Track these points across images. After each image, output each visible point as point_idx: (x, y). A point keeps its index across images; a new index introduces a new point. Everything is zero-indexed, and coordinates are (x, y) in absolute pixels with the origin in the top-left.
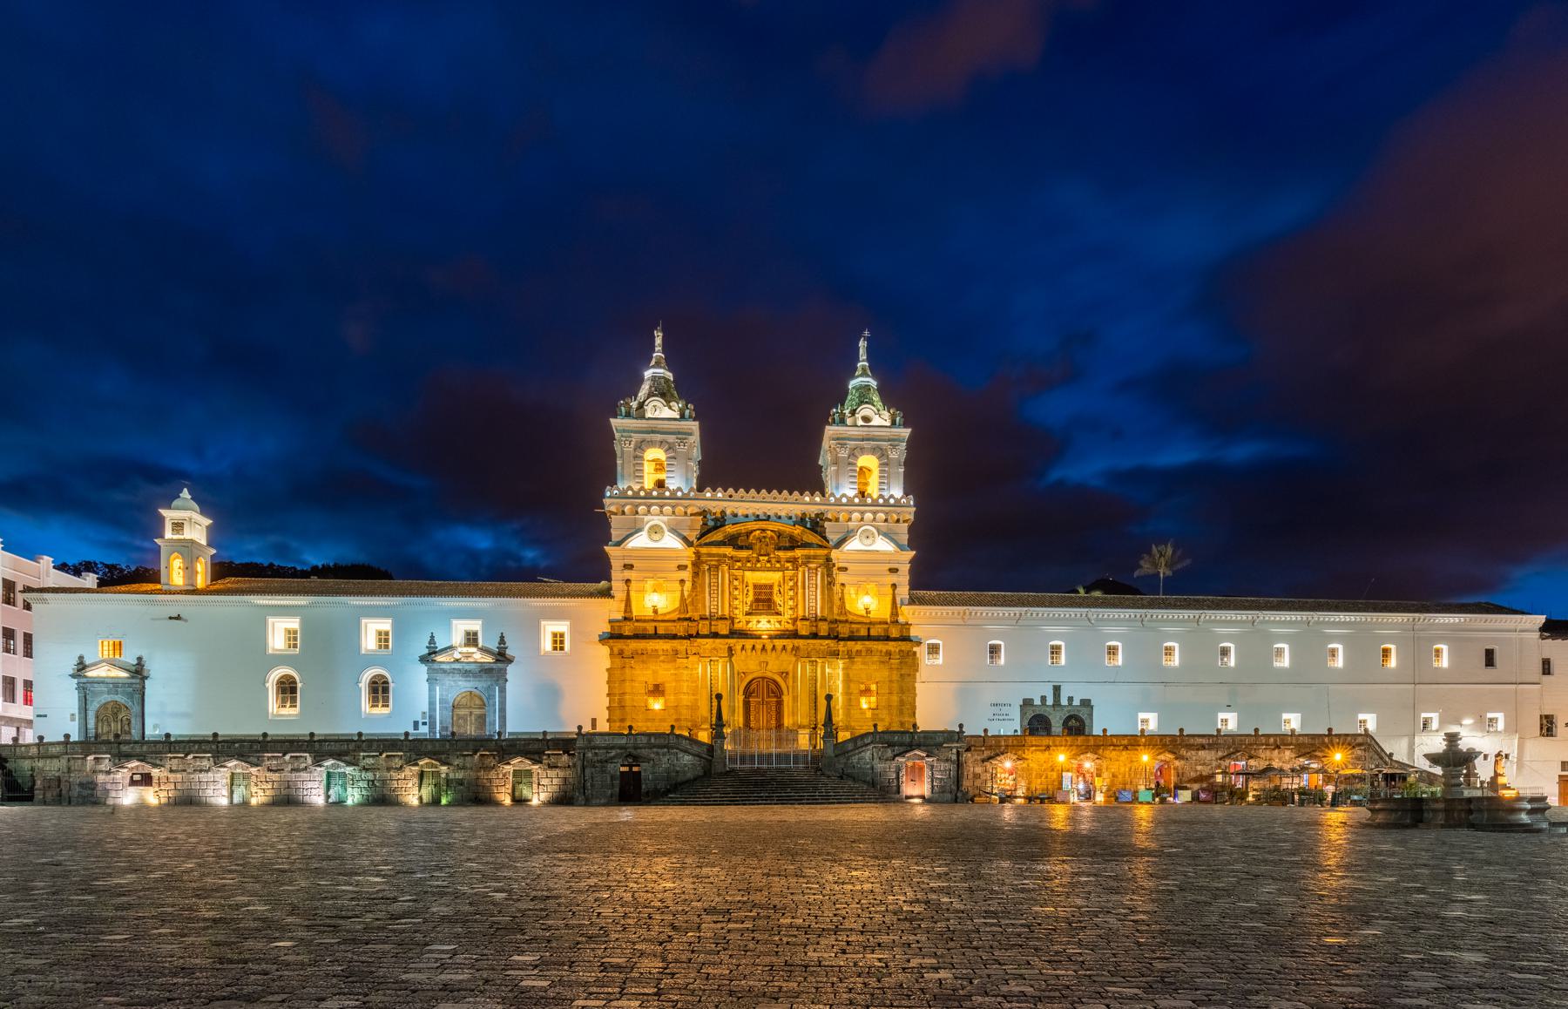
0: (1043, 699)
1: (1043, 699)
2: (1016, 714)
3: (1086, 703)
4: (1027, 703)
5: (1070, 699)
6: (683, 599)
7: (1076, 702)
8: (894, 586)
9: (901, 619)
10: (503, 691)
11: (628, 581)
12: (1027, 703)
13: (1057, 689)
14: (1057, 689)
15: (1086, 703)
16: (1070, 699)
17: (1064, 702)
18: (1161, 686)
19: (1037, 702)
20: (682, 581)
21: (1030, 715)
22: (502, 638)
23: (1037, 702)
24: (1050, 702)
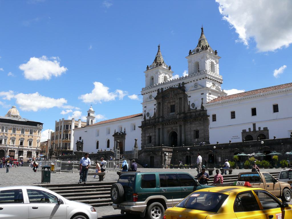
0: (250, 129)
1: (250, 129)
2: (240, 136)
3: (266, 129)
4: (244, 132)
5: (260, 128)
6: (155, 114)
7: (262, 129)
8: (202, 99)
9: (205, 109)
12: (244, 132)
13: (254, 125)
14: (254, 125)
15: (266, 129)
16: (260, 128)
17: (257, 129)
18: (277, 118)
19: (247, 131)
20: (155, 109)
21: (245, 135)
23: (247, 131)
24: (252, 130)
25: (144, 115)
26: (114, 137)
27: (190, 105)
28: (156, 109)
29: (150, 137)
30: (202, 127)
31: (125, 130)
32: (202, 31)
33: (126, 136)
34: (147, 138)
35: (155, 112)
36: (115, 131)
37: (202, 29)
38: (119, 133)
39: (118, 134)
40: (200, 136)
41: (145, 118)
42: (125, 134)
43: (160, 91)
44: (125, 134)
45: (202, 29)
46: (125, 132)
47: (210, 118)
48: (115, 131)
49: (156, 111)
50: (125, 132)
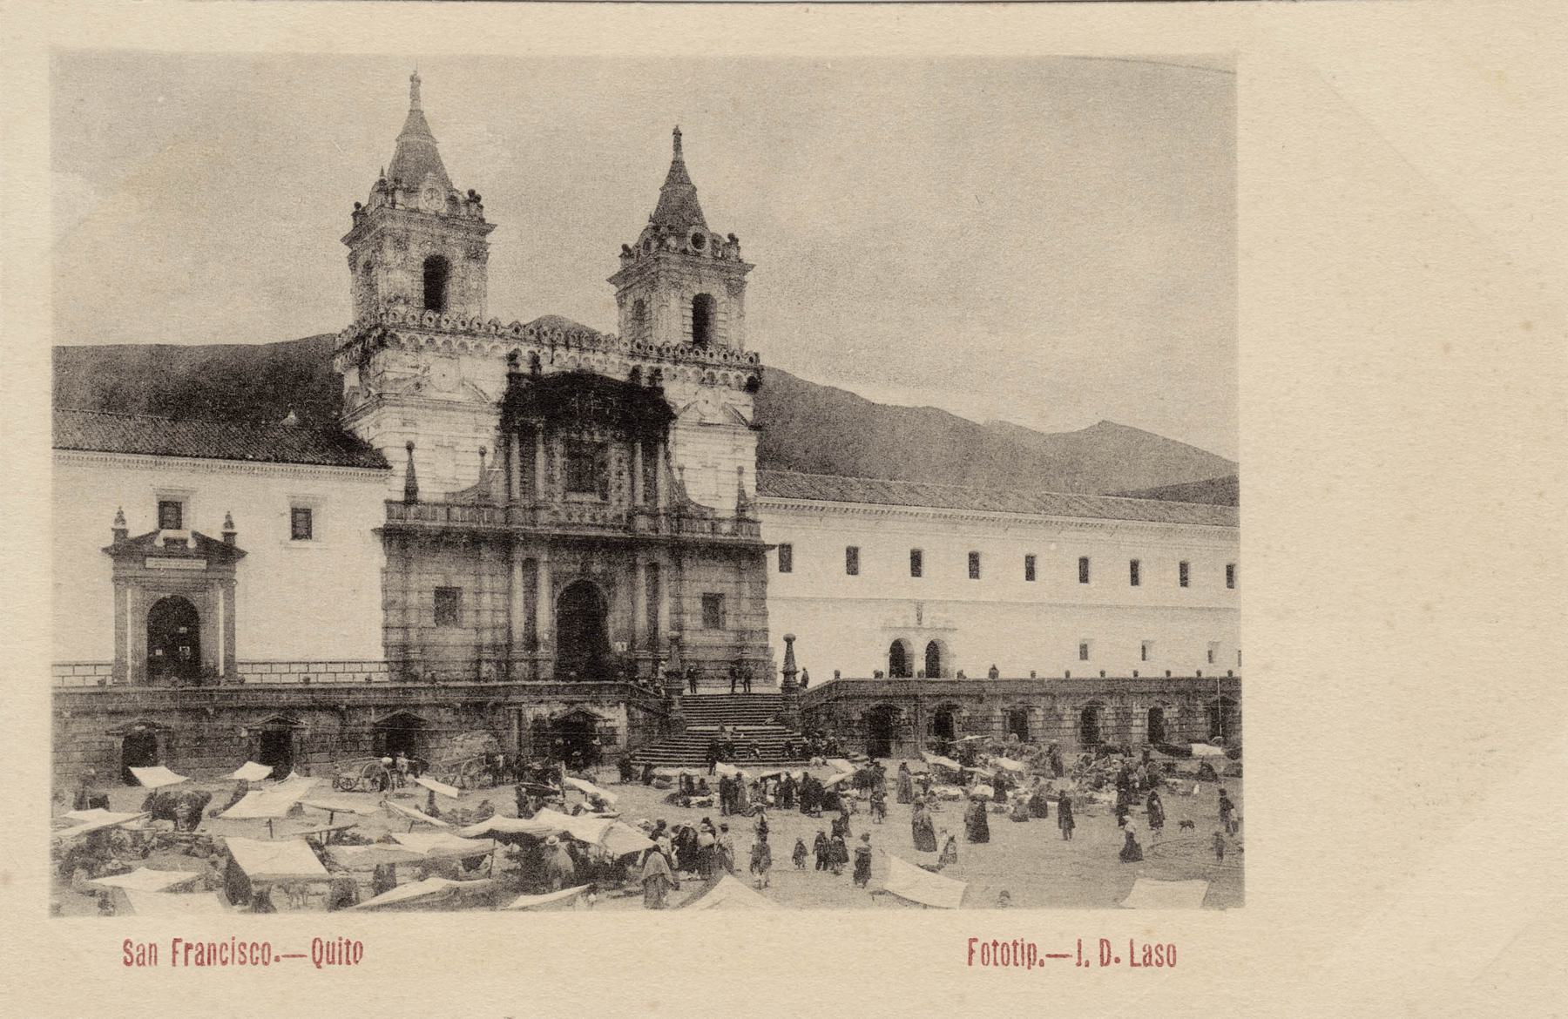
10: (230, 596)
11: (410, 448)
13: (919, 607)
14: (919, 607)
22: (228, 516)
25: (400, 468)
26: (110, 561)
27: (682, 482)
28: (490, 449)
29: (447, 599)
30: (746, 586)
31: (229, 524)
32: (677, 147)
33: (240, 568)
34: (429, 598)
35: (482, 467)
36: (120, 518)
37: (677, 134)
38: (166, 540)
39: (159, 543)
40: (730, 623)
41: (411, 491)
42: (242, 554)
43: (525, 369)
44: (242, 554)
45: (677, 134)
46: (229, 536)
47: (773, 558)
48: (120, 518)
49: (489, 459)
50: (229, 536)
